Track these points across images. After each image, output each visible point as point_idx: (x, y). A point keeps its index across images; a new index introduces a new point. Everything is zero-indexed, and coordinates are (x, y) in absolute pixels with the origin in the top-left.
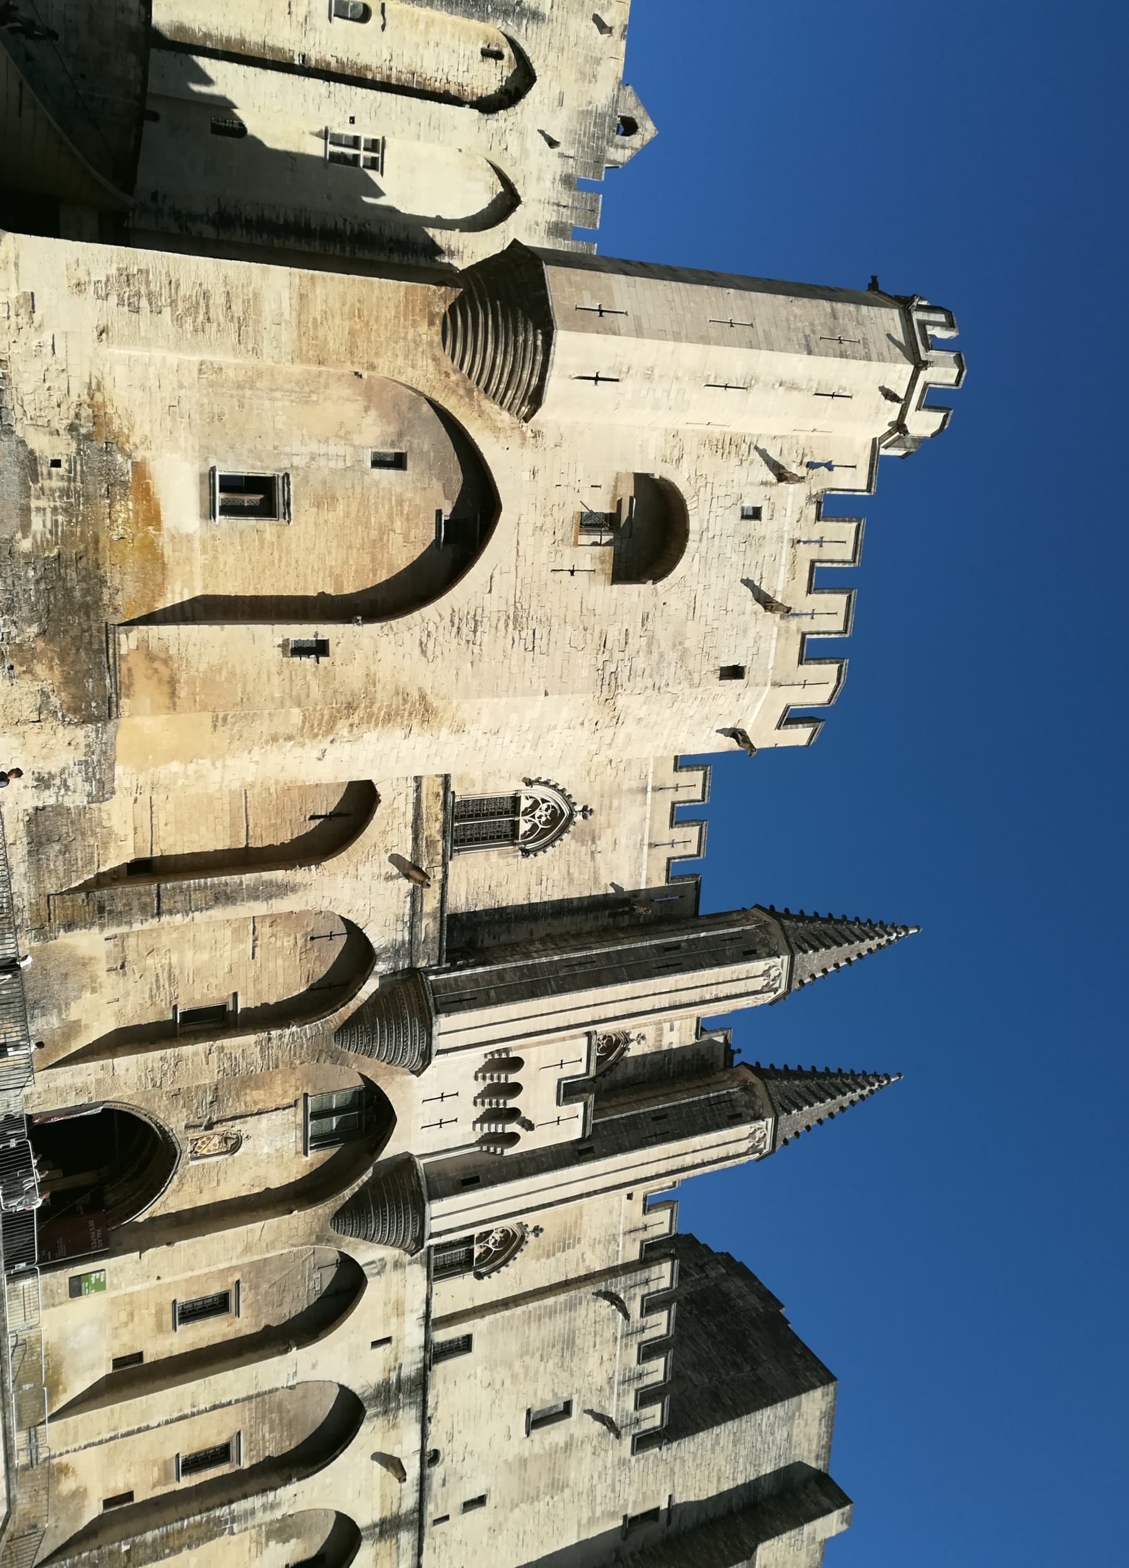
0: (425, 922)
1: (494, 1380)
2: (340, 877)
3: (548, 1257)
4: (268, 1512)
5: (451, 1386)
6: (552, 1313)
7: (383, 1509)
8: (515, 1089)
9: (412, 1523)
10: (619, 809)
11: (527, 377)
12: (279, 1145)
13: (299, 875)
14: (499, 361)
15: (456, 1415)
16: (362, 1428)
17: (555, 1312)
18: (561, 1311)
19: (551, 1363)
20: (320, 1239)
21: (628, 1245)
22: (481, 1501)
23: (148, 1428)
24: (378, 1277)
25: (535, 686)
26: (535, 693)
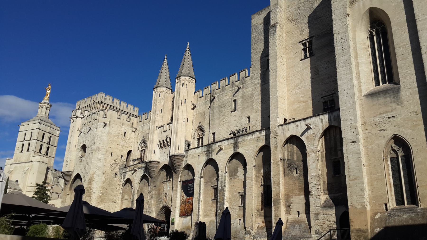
0: (143, 166)
1: (222, 124)
2: (135, 182)
3: (205, 118)
4: (223, 177)
5: (221, 135)
6: (213, 114)
7: (231, 148)
8: (163, 140)
9: (237, 139)
10: (144, 131)
11: (66, 174)
12: (168, 186)
13: (133, 190)
14: (66, 177)
15: (227, 132)
16: (213, 158)
17: (213, 113)
18: (213, 111)
19: (223, 110)
20: (178, 176)
21: (208, 98)
22: (249, 118)
23: (199, 208)
24: (187, 161)
25: (91, 163)
26: (91, 162)
